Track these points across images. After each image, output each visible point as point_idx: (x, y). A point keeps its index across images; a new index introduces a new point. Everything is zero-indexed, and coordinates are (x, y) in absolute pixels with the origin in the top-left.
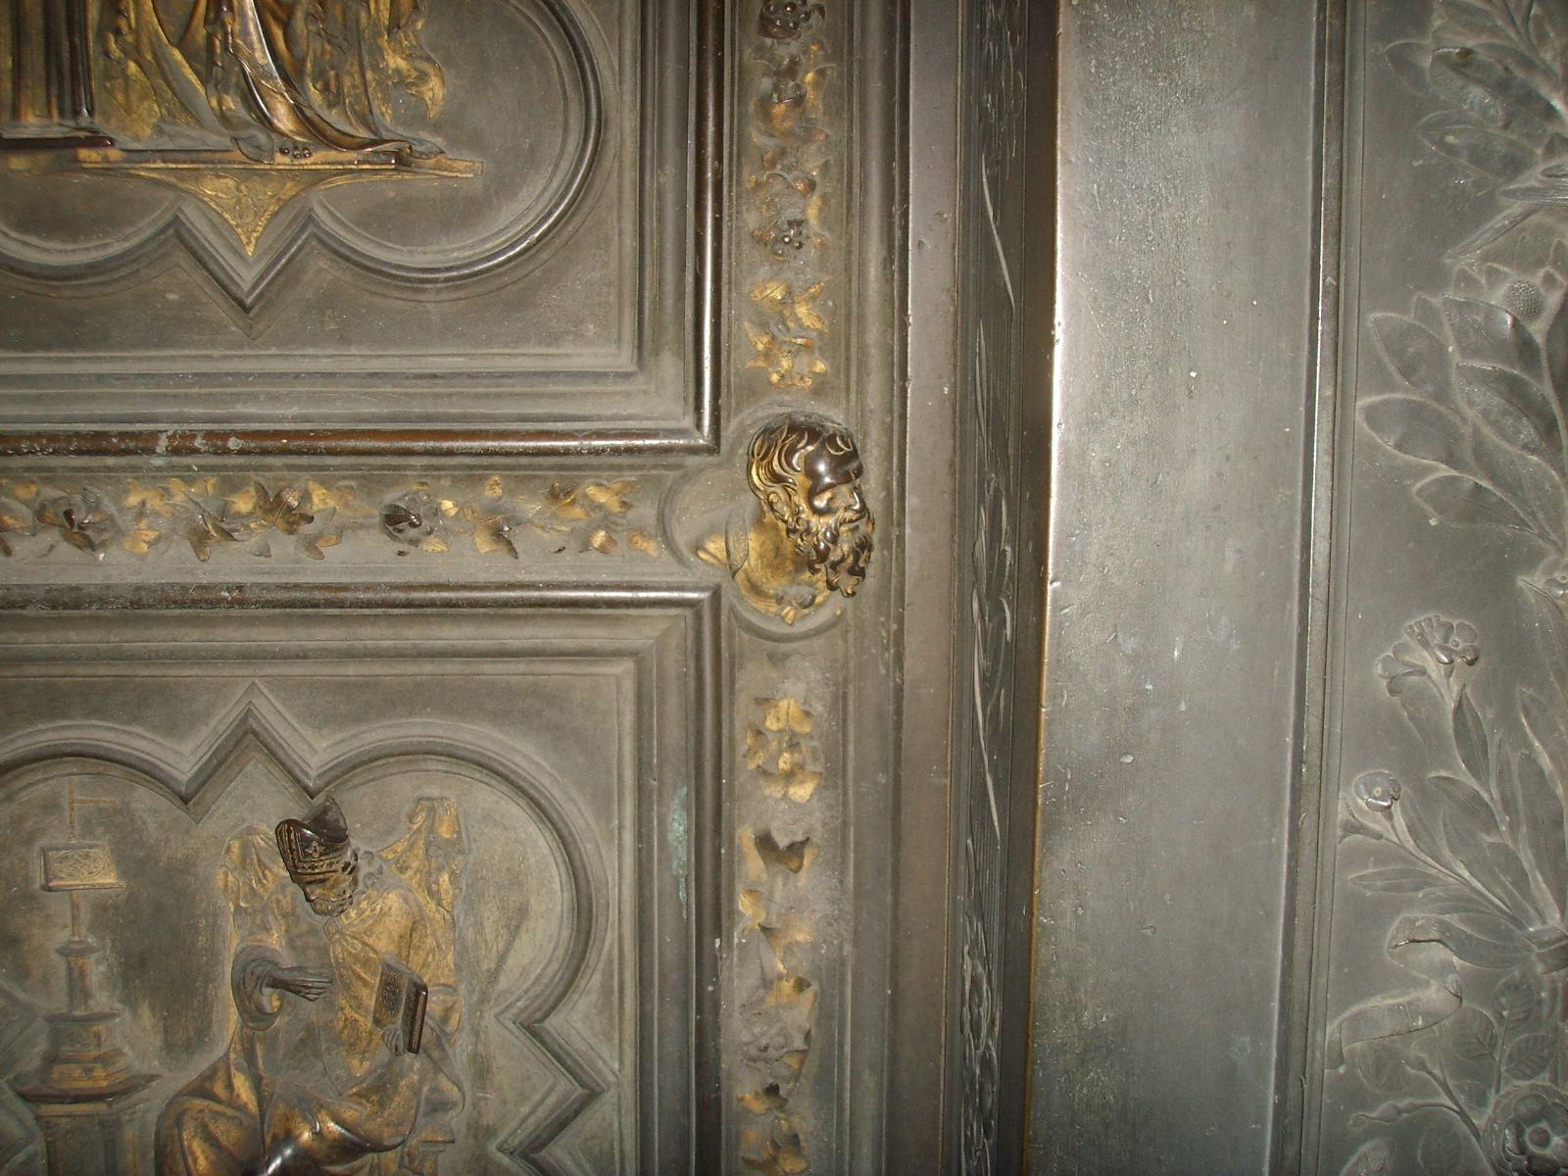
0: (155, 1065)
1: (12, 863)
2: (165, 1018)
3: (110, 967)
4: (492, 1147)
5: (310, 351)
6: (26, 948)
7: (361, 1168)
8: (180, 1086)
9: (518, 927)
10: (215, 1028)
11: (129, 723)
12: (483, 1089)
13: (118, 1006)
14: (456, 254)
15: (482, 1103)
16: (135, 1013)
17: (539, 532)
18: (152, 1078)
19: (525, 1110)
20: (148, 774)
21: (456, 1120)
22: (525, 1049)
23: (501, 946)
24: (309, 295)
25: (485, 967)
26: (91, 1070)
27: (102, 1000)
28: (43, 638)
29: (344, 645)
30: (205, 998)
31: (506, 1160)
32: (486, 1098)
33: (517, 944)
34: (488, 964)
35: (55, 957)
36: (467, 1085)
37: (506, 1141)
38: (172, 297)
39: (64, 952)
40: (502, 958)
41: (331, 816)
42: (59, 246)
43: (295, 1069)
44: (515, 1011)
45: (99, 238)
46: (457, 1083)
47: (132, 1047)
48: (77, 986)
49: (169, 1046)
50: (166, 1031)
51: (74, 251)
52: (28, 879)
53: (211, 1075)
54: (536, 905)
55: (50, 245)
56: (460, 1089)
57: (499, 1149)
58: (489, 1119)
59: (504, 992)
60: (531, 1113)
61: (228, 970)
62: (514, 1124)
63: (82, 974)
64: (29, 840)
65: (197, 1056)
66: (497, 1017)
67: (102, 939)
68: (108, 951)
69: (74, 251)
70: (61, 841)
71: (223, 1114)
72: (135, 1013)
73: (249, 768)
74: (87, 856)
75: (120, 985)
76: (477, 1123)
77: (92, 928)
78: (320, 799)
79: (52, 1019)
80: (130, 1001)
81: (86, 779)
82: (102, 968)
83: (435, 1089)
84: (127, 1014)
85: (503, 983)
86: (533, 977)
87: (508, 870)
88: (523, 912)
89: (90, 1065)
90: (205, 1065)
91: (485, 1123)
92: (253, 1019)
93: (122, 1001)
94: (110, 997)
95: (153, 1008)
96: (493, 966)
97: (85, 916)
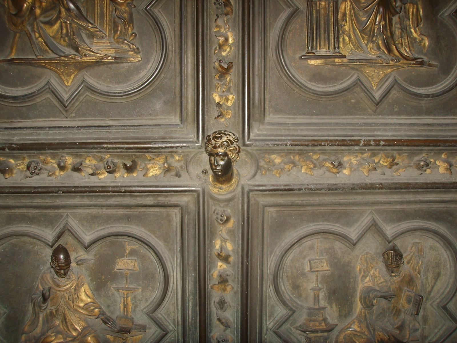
0: (336, 321)
1: (299, 265)
2: (339, 308)
3: (325, 294)
5: (390, 117)
6: (301, 288)
9: (437, 278)
10: (353, 310)
11: (335, 223)
12: (425, 325)
13: (327, 305)
14: (430, 90)
16: (331, 307)
17: (455, 168)
18: (337, 325)
19: (436, 331)
20: (344, 237)
22: (437, 314)
23: (433, 284)
24: (390, 101)
25: (428, 290)
27: (323, 303)
28: (317, 199)
29: (401, 200)
30: (351, 301)
32: (425, 328)
33: (437, 283)
34: (429, 289)
35: (309, 291)
36: (421, 324)
38: (353, 101)
39: (313, 289)
40: (433, 287)
41: (396, 248)
42: (322, 86)
44: (436, 302)
45: (333, 84)
47: (329, 316)
48: (316, 299)
49: (340, 316)
50: (339, 311)
51: (326, 87)
52: (303, 269)
54: (443, 272)
55: (319, 85)
59: (433, 297)
60: (438, 332)
61: (358, 293)
62: (433, 335)
63: (318, 296)
64: (304, 258)
66: (431, 305)
67: (323, 286)
68: (325, 289)
69: (326, 87)
70: (314, 257)
71: (357, 335)
72: (331, 307)
73: (368, 235)
74: (321, 262)
75: (327, 299)
77: (320, 283)
78: (391, 244)
79: (309, 309)
80: (330, 303)
81: (322, 239)
82: (323, 294)
83: (414, 326)
84: (329, 307)
85: (432, 294)
86: (440, 293)
87: (436, 262)
88: (439, 274)
92: (368, 307)
93: (328, 303)
94: (324, 302)
95: (336, 305)
96: (430, 290)
97: (319, 279)
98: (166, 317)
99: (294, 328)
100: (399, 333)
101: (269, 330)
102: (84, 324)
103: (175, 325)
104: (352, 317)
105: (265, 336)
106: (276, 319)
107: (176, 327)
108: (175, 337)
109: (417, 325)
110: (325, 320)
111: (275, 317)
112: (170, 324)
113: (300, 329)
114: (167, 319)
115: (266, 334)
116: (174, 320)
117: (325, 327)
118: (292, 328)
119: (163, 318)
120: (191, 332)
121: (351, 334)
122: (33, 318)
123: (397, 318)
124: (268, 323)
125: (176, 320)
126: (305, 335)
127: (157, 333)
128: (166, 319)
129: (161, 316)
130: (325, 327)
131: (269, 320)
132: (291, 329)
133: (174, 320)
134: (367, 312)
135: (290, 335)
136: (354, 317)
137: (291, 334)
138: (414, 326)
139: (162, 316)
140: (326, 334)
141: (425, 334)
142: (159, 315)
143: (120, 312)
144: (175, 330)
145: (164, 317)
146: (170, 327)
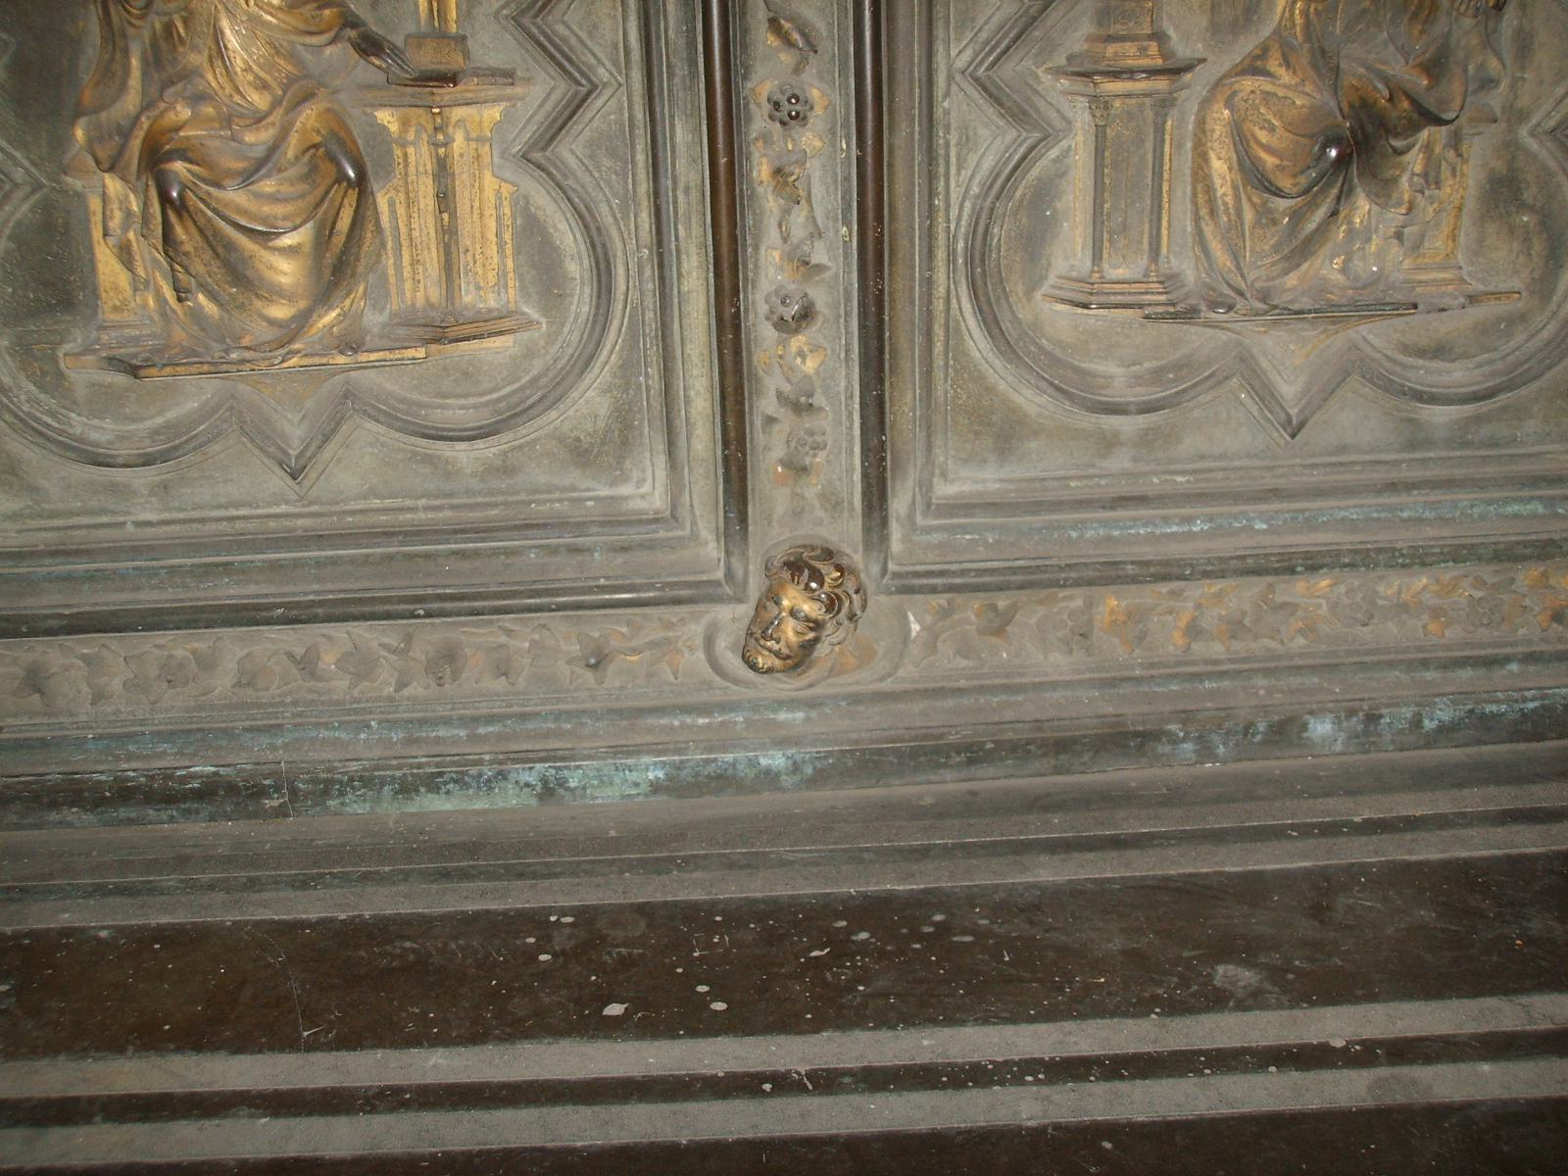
0: (1199, 49)
4: (1523, 132)
7: (1414, 145)
8: (1223, 70)
12: (1523, 68)
15: (1519, 84)
18: (1203, 61)
21: (1495, 99)
26: (1145, 49)
31: (1533, 145)
32: (1523, 79)
36: (1508, 62)
37: (1539, 124)
43: (1353, 42)
46: (1500, 59)
47: (1176, 28)
49: (1215, 28)
53: (1265, 50)
56: (1504, 66)
57: (1533, 135)
58: (1523, 102)
65: (1242, 37)
76: (1511, 107)
83: (1481, 67)
89: (1145, 44)
90: (1251, 47)
91: (1519, 105)
98: (584, 36)
99: (1048, 70)
100: (1429, 88)
101: (958, 77)
102: (289, 68)
103: (616, 63)
104: (1257, 32)
105: (944, 101)
106: (984, 35)
107: (620, 73)
108: (621, 110)
109: (1493, 64)
110: (1159, 36)
111: (980, 30)
112: (599, 61)
113: (1070, 69)
114: (589, 43)
115: (947, 94)
116: (615, 46)
117: (1160, 62)
118: (1040, 72)
119: (573, 41)
120: (677, 80)
121: (1252, 92)
122: (107, 56)
123: (1421, 32)
124: (953, 52)
125: (621, 45)
126: (1090, 89)
127: (554, 97)
128: (582, 42)
129: (567, 33)
130: (1160, 62)
131: (958, 40)
132: (1037, 77)
133: (615, 46)
134: (1312, 10)
135: (1035, 99)
136: (1266, 31)
137: (1036, 92)
138: (1481, 67)
139: (572, 31)
140: (1161, 84)
141: (1519, 104)
142: (561, 29)
143: (418, 23)
144: (620, 85)
145: (576, 35)
146: (601, 71)
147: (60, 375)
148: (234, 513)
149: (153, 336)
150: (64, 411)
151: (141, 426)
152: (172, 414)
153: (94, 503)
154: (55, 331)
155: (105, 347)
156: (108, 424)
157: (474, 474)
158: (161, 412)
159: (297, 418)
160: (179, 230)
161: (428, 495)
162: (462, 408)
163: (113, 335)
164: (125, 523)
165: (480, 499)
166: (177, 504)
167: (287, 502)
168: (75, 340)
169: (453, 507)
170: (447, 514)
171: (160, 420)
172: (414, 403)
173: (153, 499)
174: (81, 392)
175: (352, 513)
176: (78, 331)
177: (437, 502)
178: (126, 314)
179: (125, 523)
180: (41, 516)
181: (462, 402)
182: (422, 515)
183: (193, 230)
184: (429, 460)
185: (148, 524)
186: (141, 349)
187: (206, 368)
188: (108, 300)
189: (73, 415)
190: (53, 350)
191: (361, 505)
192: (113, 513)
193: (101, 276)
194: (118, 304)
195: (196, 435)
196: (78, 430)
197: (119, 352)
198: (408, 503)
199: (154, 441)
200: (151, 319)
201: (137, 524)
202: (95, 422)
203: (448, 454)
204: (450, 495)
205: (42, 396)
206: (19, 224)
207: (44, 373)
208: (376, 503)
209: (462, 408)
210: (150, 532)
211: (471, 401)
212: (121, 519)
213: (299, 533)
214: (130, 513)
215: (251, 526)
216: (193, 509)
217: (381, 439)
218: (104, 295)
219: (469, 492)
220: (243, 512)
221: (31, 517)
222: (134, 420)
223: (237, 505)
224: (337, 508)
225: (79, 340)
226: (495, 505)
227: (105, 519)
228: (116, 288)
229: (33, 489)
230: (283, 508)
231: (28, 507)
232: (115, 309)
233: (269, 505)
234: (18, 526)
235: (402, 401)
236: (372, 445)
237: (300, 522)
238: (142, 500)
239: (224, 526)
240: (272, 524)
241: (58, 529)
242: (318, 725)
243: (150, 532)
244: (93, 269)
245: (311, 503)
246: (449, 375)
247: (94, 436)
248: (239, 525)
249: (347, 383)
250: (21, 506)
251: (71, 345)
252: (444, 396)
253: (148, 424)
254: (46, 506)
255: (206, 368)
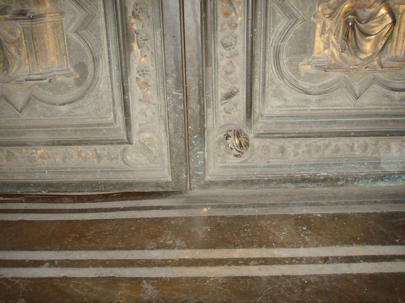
147: (299, 70)
148: (336, 108)
149: (327, 61)
150: (297, 80)
151: (316, 84)
152: (324, 82)
153: (300, 104)
154: (300, 58)
155: (314, 63)
156: (308, 83)
157: (398, 100)
158: (322, 81)
159: (357, 84)
160: (350, 33)
161: (385, 105)
162: (399, 83)
163: (316, 60)
164: (307, 110)
165: (398, 107)
166: (322, 105)
167: (350, 106)
168: (304, 61)
169: (392, 109)
170: (390, 110)
171: (321, 83)
172: (387, 82)
173: (316, 104)
174: (303, 75)
175: (366, 109)
176: (306, 59)
177: (388, 107)
178: (320, 55)
179: (307, 110)
180: (286, 107)
181: (399, 82)
182: (383, 110)
183: (353, 33)
184: (388, 96)
185: (314, 110)
186: (324, 64)
187: (344, 70)
188: (316, 51)
189: (299, 81)
190: (298, 63)
191: (368, 107)
192: (305, 107)
193: (316, 45)
194: (319, 52)
195: (334, 87)
196: (300, 85)
197: (318, 65)
198: (380, 107)
199: (320, 89)
200: (327, 57)
201: (311, 110)
202: (305, 83)
203: (393, 95)
204: (390, 105)
205: (292, 76)
206: (296, 30)
207: (294, 70)
208: (372, 107)
209: (399, 83)
210: (314, 112)
211: (401, 81)
212: (307, 108)
213: (353, 114)
214: (309, 107)
215: (340, 111)
216: (326, 106)
217: (377, 90)
218: (315, 50)
219: (396, 105)
220: (338, 108)
221: (283, 107)
222: (315, 83)
223: (337, 106)
224: (362, 108)
225: (306, 61)
226: (401, 108)
227: (302, 108)
228: (319, 48)
229: (285, 100)
230: (349, 107)
231: (283, 104)
232: (318, 53)
233: (345, 106)
234: (279, 109)
235: (385, 81)
236: (374, 92)
237: (352, 111)
238: (313, 104)
239: (333, 111)
240: (345, 111)
241: (290, 110)
242: (351, 164)
243: (314, 112)
244: (314, 42)
245: (356, 106)
246: (397, 75)
247: (304, 86)
248: (337, 111)
249: (374, 76)
250: (281, 104)
251: (303, 62)
252: (394, 80)
253: (318, 84)
254: (288, 104)
255: (344, 70)
